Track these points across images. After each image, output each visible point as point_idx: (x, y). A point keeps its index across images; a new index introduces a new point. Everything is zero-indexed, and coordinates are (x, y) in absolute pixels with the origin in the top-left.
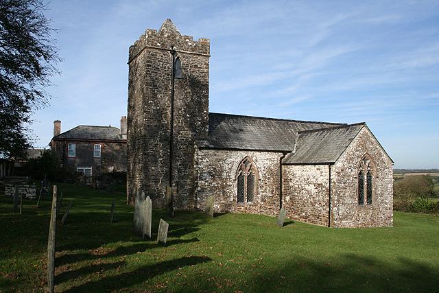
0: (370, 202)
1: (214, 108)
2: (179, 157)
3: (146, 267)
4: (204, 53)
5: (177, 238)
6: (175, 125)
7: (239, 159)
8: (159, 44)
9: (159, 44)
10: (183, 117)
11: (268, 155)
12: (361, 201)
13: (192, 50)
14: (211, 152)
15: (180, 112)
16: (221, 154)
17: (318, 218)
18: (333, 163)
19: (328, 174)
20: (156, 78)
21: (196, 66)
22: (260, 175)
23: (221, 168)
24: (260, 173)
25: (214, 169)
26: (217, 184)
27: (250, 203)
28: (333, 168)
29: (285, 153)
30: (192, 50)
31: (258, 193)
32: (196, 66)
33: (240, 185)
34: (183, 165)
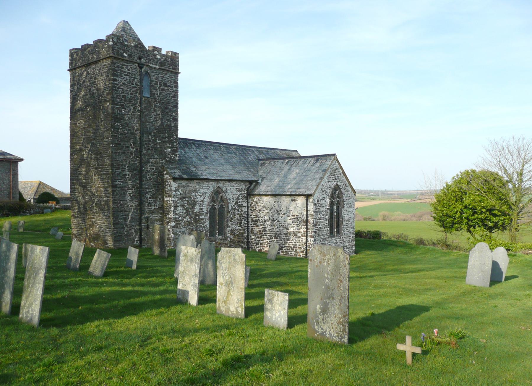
0: (338, 232)
1: (183, 133)
2: (148, 189)
3: (369, 337)
4: (173, 69)
5: (163, 280)
6: (144, 152)
7: (211, 190)
8: (125, 54)
9: (125, 54)
10: (153, 143)
11: (237, 186)
12: (332, 232)
13: (162, 64)
14: (184, 183)
15: (150, 137)
16: (193, 185)
17: (293, 250)
18: (311, 195)
19: (305, 209)
20: (123, 96)
21: (165, 84)
22: (230, 207)
23: (194, 200)
24: (230, 205)
25: (188, 201)
26: (191, 218)
27: (221, 237)
28: (311, 200)
29: (251, 182)
30: (162, 64)
31: (228, 226)
32: (165, 84)
33: (212, 218)
34: (153, 198)
